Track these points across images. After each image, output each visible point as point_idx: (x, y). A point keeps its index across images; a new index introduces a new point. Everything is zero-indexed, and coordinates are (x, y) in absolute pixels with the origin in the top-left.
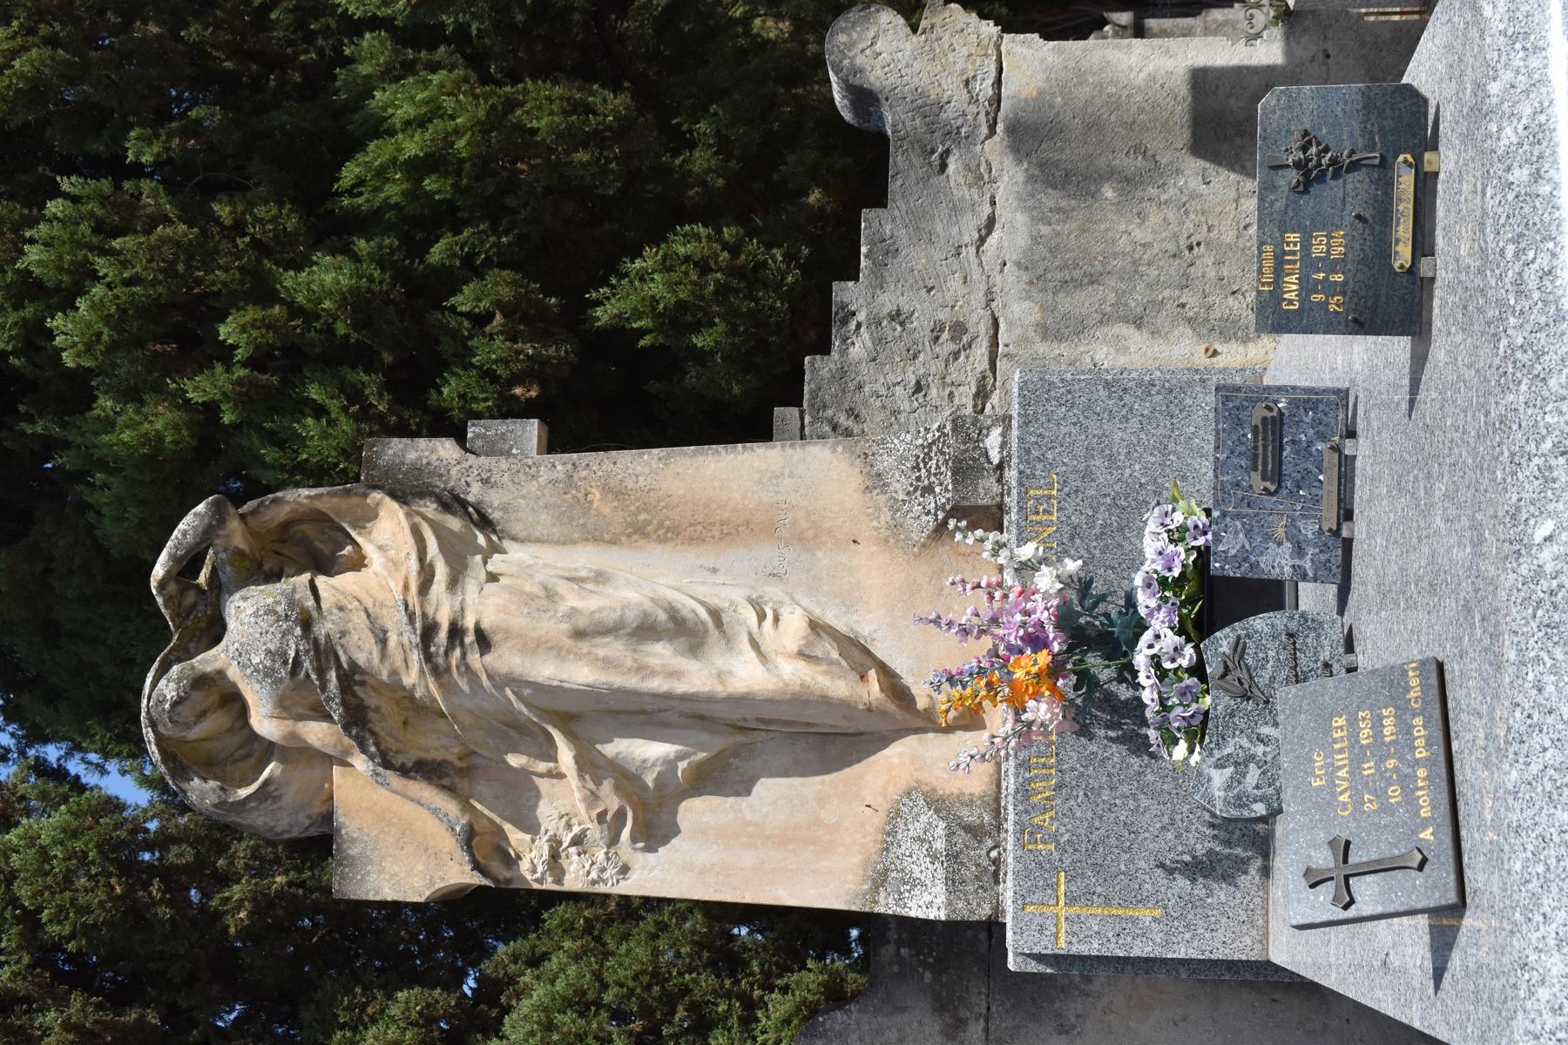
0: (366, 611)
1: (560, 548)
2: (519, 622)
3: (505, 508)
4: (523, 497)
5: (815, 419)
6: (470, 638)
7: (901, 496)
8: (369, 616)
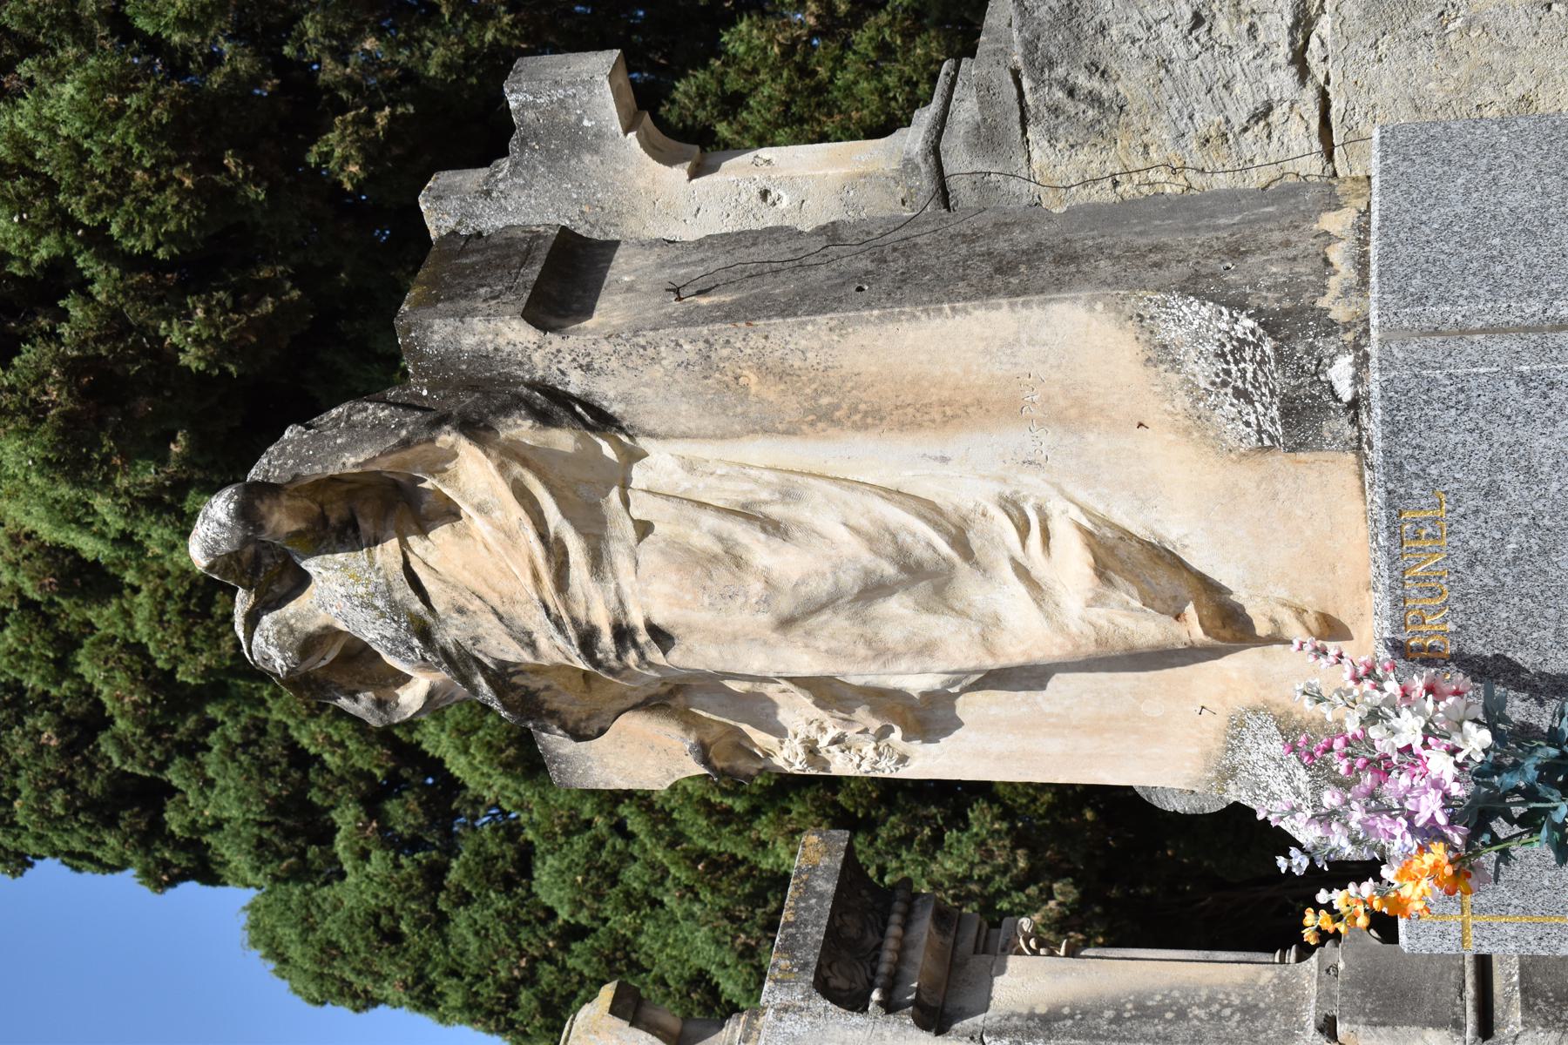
0: (496, 612)
1: (719, 443)
2: (702, 617)
3: (626, 399)
4: (647, 385)
5: (1038, 83)
6: (643, 637)
7: (1203, 384)
8: (501, 618)
